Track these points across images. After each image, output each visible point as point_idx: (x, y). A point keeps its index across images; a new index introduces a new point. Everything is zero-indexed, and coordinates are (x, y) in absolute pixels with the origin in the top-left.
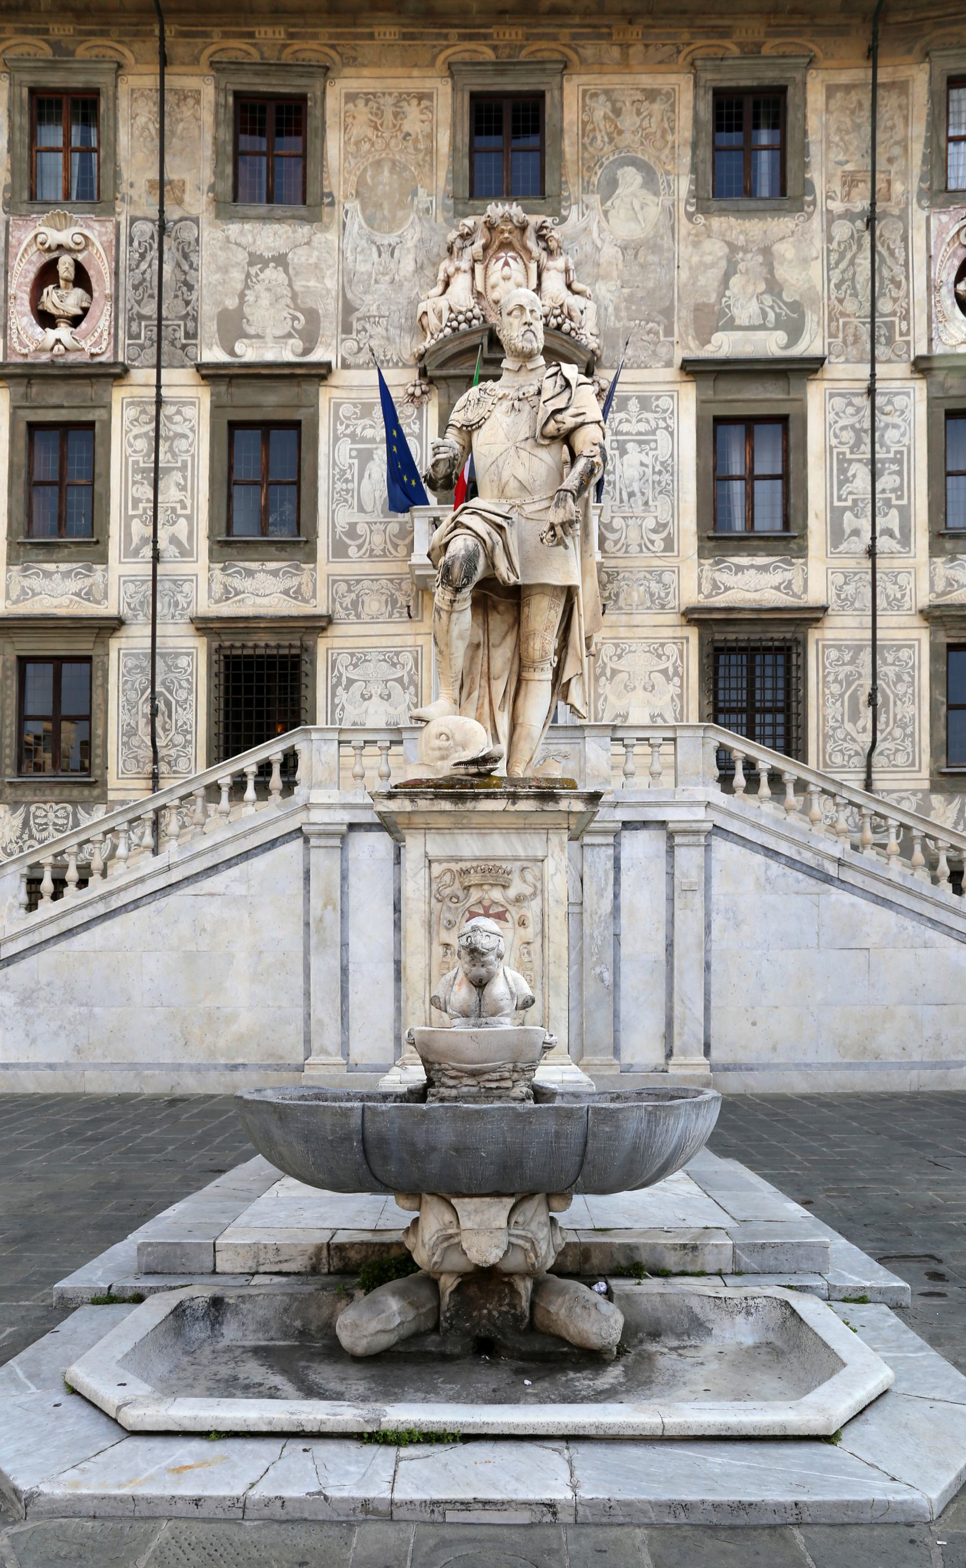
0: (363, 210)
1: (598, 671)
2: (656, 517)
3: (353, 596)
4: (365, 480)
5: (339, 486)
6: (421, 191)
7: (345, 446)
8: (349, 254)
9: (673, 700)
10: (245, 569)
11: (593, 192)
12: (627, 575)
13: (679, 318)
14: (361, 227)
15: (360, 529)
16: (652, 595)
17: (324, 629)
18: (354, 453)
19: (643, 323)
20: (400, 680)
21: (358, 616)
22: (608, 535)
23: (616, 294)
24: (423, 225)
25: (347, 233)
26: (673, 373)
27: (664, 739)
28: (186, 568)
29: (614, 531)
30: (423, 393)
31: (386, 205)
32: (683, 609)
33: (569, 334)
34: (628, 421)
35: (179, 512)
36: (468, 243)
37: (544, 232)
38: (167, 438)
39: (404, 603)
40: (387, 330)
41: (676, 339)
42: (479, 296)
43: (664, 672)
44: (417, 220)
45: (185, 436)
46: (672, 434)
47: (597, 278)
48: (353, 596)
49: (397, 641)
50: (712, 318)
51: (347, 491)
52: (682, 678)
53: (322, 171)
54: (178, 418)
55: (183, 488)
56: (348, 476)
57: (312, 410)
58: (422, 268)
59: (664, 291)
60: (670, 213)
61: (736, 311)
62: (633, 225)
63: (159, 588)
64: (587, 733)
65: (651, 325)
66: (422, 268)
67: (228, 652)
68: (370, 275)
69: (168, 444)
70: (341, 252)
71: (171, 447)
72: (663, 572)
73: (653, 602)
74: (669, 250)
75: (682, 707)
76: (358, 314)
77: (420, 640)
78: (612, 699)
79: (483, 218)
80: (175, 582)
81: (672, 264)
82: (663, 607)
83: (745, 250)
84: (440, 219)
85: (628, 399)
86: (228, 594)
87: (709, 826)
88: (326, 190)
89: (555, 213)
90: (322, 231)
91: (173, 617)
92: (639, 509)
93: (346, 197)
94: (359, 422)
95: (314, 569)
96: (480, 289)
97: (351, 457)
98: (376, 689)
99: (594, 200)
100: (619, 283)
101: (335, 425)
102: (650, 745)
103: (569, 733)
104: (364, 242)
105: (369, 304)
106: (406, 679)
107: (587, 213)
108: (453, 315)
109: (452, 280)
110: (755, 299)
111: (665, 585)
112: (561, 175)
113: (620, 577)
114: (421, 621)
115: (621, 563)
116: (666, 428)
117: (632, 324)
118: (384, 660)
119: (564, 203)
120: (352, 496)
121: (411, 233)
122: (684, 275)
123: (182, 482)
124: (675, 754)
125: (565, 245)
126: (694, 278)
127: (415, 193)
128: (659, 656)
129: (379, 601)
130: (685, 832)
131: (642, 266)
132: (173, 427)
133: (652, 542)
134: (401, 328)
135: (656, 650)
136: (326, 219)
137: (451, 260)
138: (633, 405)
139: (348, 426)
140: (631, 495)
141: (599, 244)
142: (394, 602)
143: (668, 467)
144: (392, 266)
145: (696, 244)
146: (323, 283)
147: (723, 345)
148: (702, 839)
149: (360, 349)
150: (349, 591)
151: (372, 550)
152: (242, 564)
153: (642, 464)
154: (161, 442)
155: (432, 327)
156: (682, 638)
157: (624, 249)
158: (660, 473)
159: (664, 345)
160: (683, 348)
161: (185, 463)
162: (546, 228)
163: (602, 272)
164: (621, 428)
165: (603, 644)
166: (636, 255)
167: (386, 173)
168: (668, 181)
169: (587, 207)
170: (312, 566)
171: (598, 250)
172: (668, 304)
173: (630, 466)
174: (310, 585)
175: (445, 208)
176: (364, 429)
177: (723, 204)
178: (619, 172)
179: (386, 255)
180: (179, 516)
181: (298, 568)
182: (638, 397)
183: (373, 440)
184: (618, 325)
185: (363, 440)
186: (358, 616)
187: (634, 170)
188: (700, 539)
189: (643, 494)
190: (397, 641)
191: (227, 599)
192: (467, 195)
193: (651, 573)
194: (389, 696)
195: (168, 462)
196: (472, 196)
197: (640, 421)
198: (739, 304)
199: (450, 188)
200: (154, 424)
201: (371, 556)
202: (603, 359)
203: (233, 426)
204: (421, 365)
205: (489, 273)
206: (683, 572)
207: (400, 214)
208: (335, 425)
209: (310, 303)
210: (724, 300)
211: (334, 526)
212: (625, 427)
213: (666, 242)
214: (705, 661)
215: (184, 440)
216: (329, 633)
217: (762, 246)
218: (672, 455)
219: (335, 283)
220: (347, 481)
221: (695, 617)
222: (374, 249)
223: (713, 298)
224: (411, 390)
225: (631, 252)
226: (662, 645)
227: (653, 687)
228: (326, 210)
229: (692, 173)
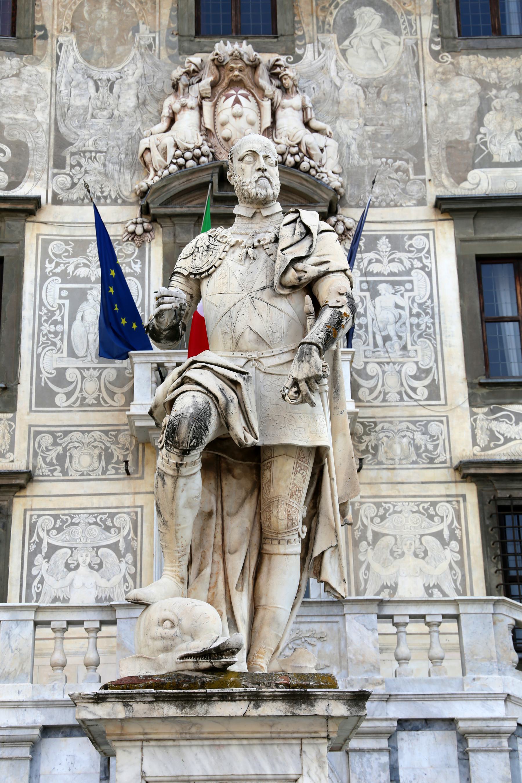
0: (79, 44)
1: (357, 534)
2: (417, 363)
3: (60, 449)
4: (77, 323)
6: (142, 28)
8: (62, 88)
9: (451, 568)
11: (329, 32)
12: (386, 425)
13: (430, 156)
14: (76, 61)
15: (70, 375)
16: (417, 448)
17: (22, 487)
18: (65, 293)
19: (390, 161)
20: (114, 547)
21: (65, 472)
22: (361, 381)
23: (360, 132)
24: (145, 62)
25: (61, 66)
26: (426, 211)
27: (444, 616)
29: (369, 378)
30: (145, 231)
31: (104, 40)
32: (456, 463)
33: (308, 172)
34: (378, 261)
36: (194, 80)
37: (278, 70)
39: (121, 458)
40: (104, 165)
41: (427, 176)
42: (207, 133)
43: (439, 535)
44: (138, 56)
46: (429, 274)
47: (337, 116)
48: (60, 449)
49: (112, 501)
50: (467, 155)
51: (56, 333)
52: (460, 542)
53: (34, 5)
57: (17, 246)
58: (144, 103)
59: (411, 129)
60: (414, 51)
61: (493, 148)
62: (374, 64)
64: (347, 609)
65: (398, 163)
66: (144, 103)
68: (86, 109)
70: (54, 85)
72: (429, 422)
73: (419, 455)
74: (415, 88)
75: (463, 576)
76: (71, 149)
77: (140, 500)
78: (376, 567)
79: (211, 56)
81: (419, 101)
82: (431, 461)
83: (499, 87)
84: (164, 56)
85: (377, 238)
87: (512, 726)
88: (37, 23)
89: (289, 51)
90: (32, 64)
92: (396, 354)
93: (60, 31)
94: (71, 260)
95: (13, 419)
96: (209, 125)
97: (61, 297)
98: (84, 557)
99: (331, 39)
100: (361, 121)
102: (428, 624)
103: (325, 610)
104: (79, 77)
105: (85, 138)
106: (122, 546)
107: (323, 52)
108: (179, 152)
109: (178, 117)
110: (513, 136)
111: (432, 437)
112: (294, 15)
113: (377, 429)
114: (142, 478)
115: (379, 412)
116: (423, 268)
117: (378, 162)
118: (96, 523)
119: (298, 42)
120: (62, 340)
121: (132, 69)
122: (433, 112)
124: (460, 633)
125: (302, 83)
126: (444, 116)
127: (136, 30)
128: (431, 517)
129: (91, 455)
130: (481, 734)
131: (385, 104)
133: (414, 390)
134: (120, 164)
135: (427, 510)
136: (37, 52)
137: (176, 96)
138: (384, 245)
139: (58, 264)
140: (386, 339)
141: (338, 82)
142: (109, 457)
143: (428, 309)
144: (111, 101)
145: (444, 82)
146: (33, 116)
147: (481, 182)
148: (505, 743)
149: (74, 185)
150: (55, 444)
151: (84, 399)
153: (397, 306)
155: (156, 164)
156: (457, 496)
157: (365, 87)
158: (418, 315)
159: (414, 183)
160: (437, 186)
162: (280, 66)
163: (342, 110)
164: (371, 268)
165: (361, 503)
166: (379, 93)
167: (105, 9)
168: (409, 21)
169: (323, 46)
170: (10, 415)
171: (338, 88)
172: (416, 141)
173: (383, 308)
175: (169, 45)
176: (77, 267)
177: (471, 43)
178: (357, 12)
179: (104, 90)
182: (388, 236)
183: (87, 280)
184: (362, 163)
185: (76, 279)
186: (65, 472)
187: (372, 10)
188: (470, 385)
189: (400, 338)
190: (112, 501)
192: (193, 32)
193: (414, 423)
194: (101, 565)
196: (198, 33)
197: (392, 261)
198: (496, 141)
199: (174, 25)
201: (82, 405)
202: (347, 196)
204: (143, 202)
205: (219, 110)
206: (453, 422)
207: (120, 49)
209: (18, 135)
210: (479, 137)
211: (39, 372)
212: (375, 268)
213: (411, 80)
214: (488, 522)
216: (28, 492)
217: (516, 83)
218: (431, 297)
219: (46, 116)
220: (55, 323)
221: (469, 471)
222: (91, 83)
223: (466, 135)
224: (131, 228)
225: (373, 91)
226: (434, 504)
227: (426, 552)
228: (38, 43)
229: (434, 12)
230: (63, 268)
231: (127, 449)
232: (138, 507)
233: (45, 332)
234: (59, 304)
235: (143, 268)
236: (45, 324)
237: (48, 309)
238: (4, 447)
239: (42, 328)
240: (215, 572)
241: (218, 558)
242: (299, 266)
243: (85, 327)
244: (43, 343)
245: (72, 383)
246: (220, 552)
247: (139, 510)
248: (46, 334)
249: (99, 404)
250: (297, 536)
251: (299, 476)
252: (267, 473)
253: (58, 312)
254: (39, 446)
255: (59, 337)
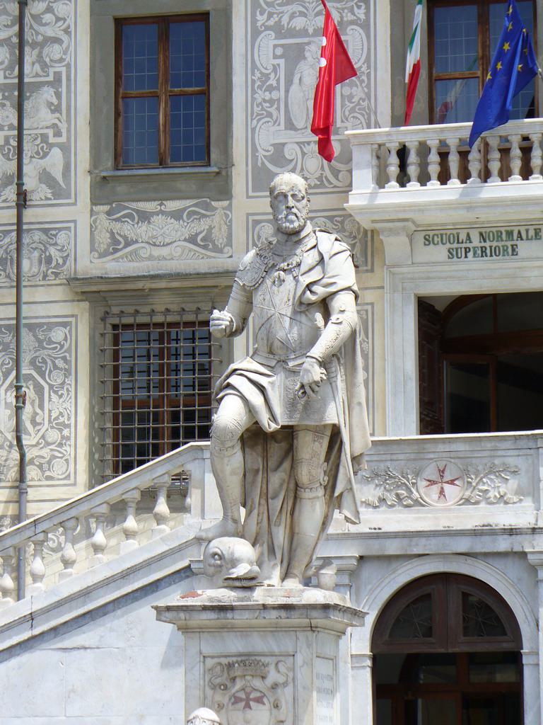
4: (295, 88)
5: (261, 95)
7: (268, 42)
10: (137, 211)
18: (279, 51)
28: (58, 214)
35: (52, 140)
38: (34, 45)
45: (57, 40)
51: (271, 102)
54: (48, 17)
55: (56, 109)
56: (272, 82)
63: (26, 240)
67: (116, 321)
69: (36, 52)
71: (40, 55)
80: (45, 231)
86: (116, 244)
91: (45, 277)
95: (229, 208)
97: (275, 57)
101: (254, 15)
114: (372, 270)
120: (278, 109)
123: (55, 101)
132: (41, 29)
139: (270, 15)
152: (134, 205)
154: (27, 49)
161: (58, 76)
170: (226, 203)
174: (224, 228)
176: (292, 17)
180: (51, 146)
181: (207, 207)
183: (304, 32)
185: (292, 33)
191: (116, 251)
195: (37, 75)
200: (16, 28)
203: (120, 23)
208: (254, 15)
211: (255, 150)
215: (56, 46)
230: (277, 19)
231: (355, 237)
232: (367, 304)
233: (259, 100)
234: (273, 65)
235: (367, 14)
236: (259, 92)
237: (261, 73)
238: (221, 241)
239: (256, 96)
240: (261, 512)
241: (263, 502)
242: (315, 288)
243: (304, 92)
244: (258, 115)
245: (293, 160)
246: (265, 497)
247: (369, 308)
248: (260, 104)
249: (322, 185)
250: (319, 484)
251: (316, 443)
252: (295, 441)
253: (272, 76)
254: (259, 237)
255: (276, 106)
